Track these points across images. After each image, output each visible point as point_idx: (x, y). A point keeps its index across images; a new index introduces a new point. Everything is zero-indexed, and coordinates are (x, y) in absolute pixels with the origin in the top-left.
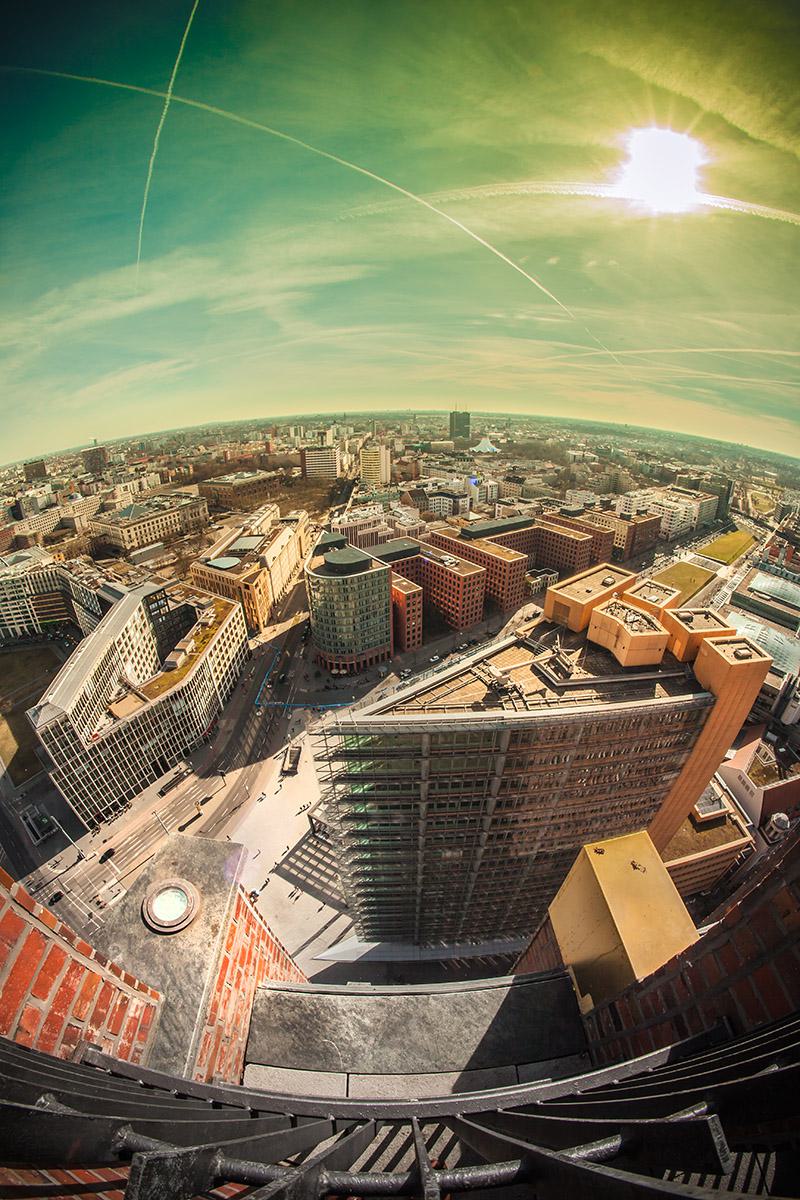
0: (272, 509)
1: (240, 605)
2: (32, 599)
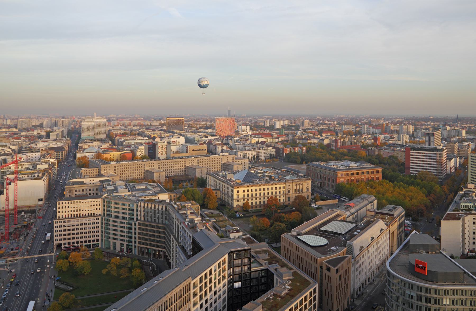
0: (370, 200)
1: (317, 286)
2: (139, 224)
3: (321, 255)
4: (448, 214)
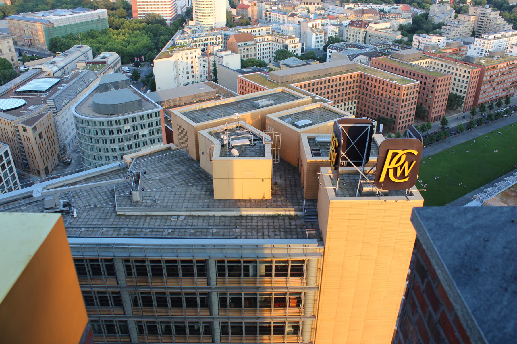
1: (8, 148)
3: (16, 118)
4: (163, 53)
